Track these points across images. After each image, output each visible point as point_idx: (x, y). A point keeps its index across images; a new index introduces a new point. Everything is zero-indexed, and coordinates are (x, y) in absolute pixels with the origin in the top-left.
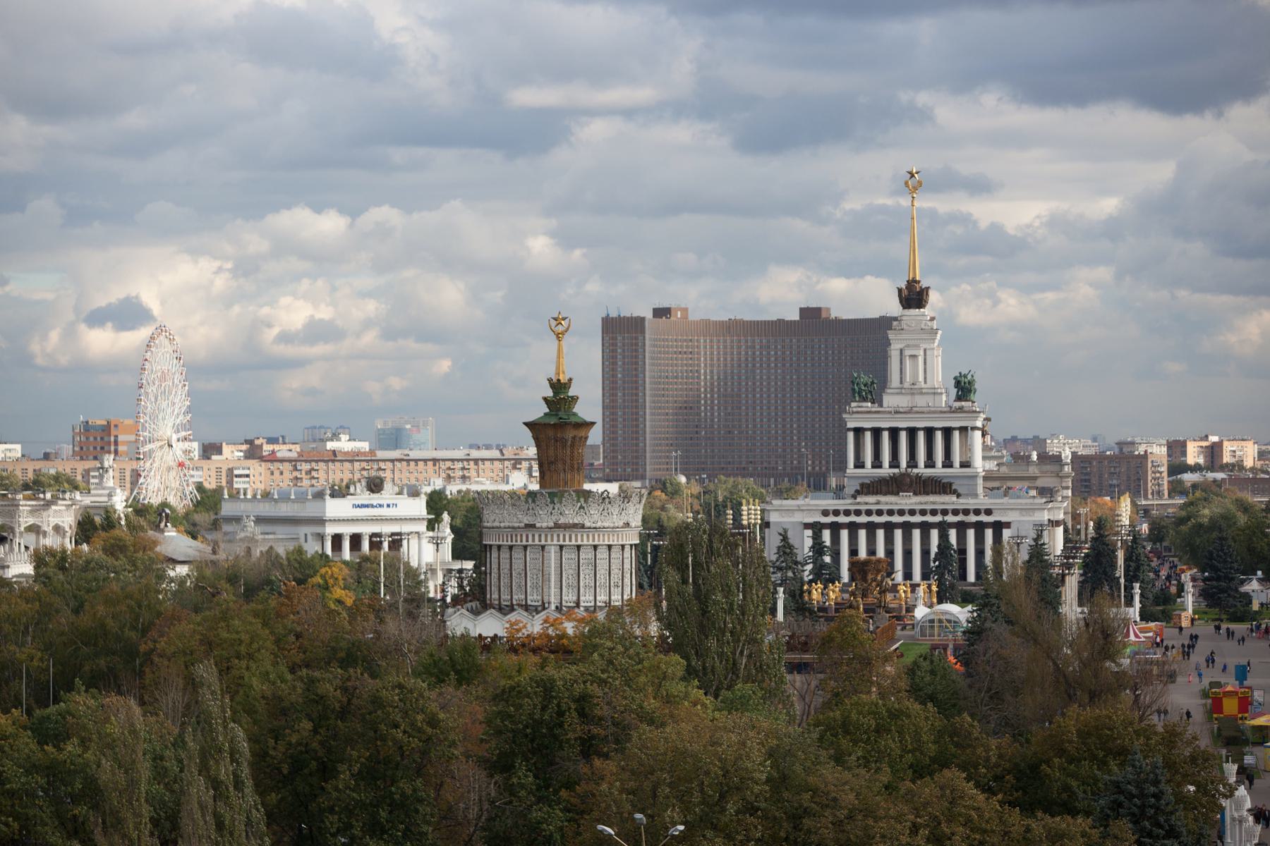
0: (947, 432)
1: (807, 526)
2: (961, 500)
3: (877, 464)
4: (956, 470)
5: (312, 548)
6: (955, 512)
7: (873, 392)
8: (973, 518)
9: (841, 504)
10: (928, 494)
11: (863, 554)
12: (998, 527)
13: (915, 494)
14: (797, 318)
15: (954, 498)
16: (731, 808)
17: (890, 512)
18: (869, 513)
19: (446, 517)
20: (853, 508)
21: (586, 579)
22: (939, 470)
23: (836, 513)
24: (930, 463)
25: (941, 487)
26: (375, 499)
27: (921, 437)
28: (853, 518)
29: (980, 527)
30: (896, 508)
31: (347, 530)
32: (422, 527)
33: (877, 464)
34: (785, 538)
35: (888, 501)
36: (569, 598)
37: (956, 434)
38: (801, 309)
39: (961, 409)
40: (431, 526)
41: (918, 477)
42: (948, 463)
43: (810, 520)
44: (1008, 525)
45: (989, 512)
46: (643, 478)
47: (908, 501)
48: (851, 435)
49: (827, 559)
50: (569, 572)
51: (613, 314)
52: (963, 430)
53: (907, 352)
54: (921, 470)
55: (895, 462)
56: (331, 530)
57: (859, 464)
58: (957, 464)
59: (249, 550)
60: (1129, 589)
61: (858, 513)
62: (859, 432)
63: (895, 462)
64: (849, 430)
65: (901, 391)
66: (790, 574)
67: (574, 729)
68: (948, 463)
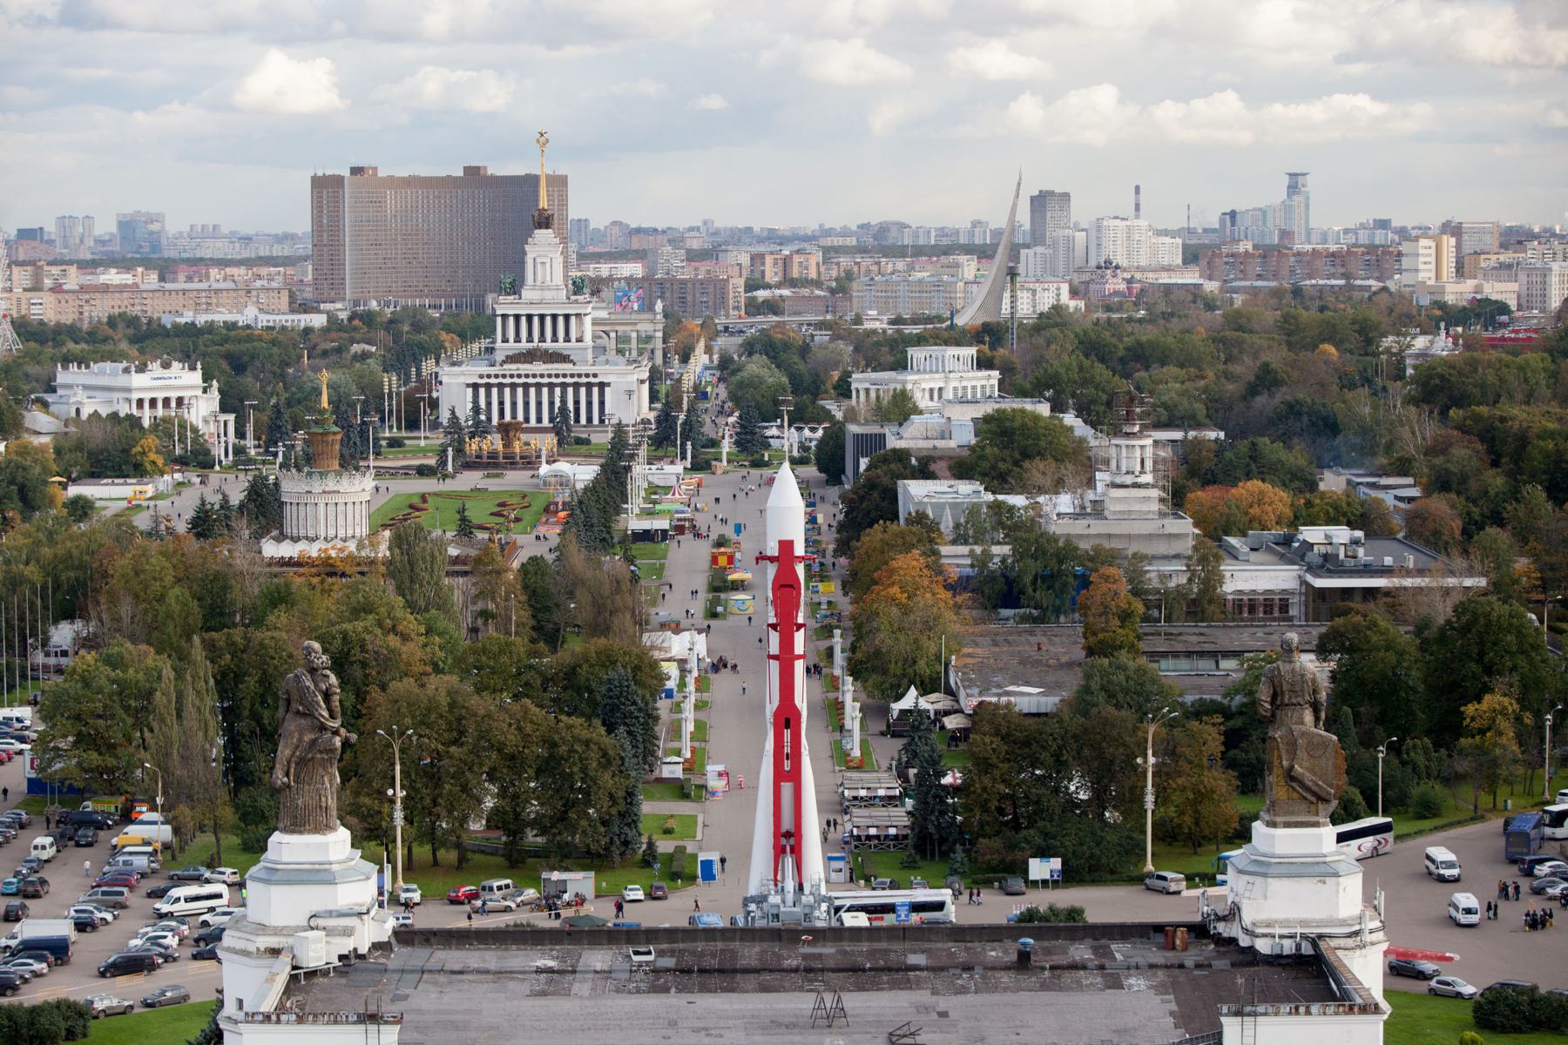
0: (567, 317)
1: (468, 385)
3: (517, 340)
4: (573, 344)
5: (123, 410)
6: (572, 376)
7: (515, 288)
8: (584, 380)
9: (492, 371)
11: (508, 418)
12: (602, 386)
14: (461, 174)
16: (433, 717)
17: (527, 376)
18: (512, 376)
19: (215, 383)
21: (341, 521)
22: (560, 345)
23: (489, 376)
24: (555, 339)
25: (565, 359)
26: (166, 373)
27: (548, 320)
28: (500, 380)
29: (589, 386)
31: (147, 396)
32: (199, 392)
33: (517, 340)
34: (453, 412)
35: (525, 368)
36: (331, 533)
37: (573, 319)
38: (466, 169)
39: (576, 302)
40: (205, 391)
41: (546, 351)
42: (567, 339)
44: (609, 384)
45: (595, 376)
46: (344, 299)
47: (538, 367)
48: (499, 320)
49: (483, 417)
50: (331, 518)
51: (320, 174)
53: (539, 260)
54: (548, 345)
55: (530, 340)
56: (135, 396)
57: (505, 340)
59: (78, 411)
60: (683, 445)
61: (504, 376)
62: (505, 317)
63: (530, 340)
65: (534, 288)
67: (356, 654)
68: (567, 339)
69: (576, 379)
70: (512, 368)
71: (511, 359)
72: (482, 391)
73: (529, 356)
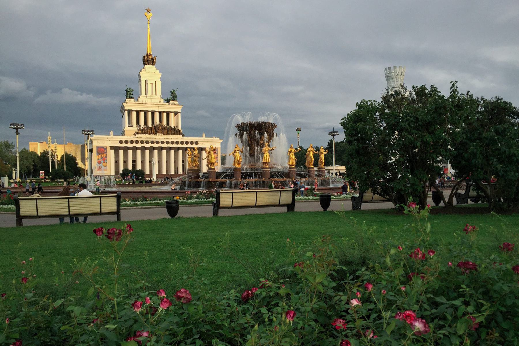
0: (168, 113)
1: (112, 148)
2: (184, 138)
6: (182, 143)
10: (169, 134)
13: (164, 134)
15: (181, 136)
17: (152, 142)
18: (142, 142)
20: (134, 140)
28: (134, 145)
30: (155, 140)
43: (114, 145)
44: (205, 149)
45: (197, 143)
47: (160, 137)
48: (126, 112)
53: (148, 82)
61: (137, 142)
64: (125, 110)
69: (185, 145)
72: (121, 152)
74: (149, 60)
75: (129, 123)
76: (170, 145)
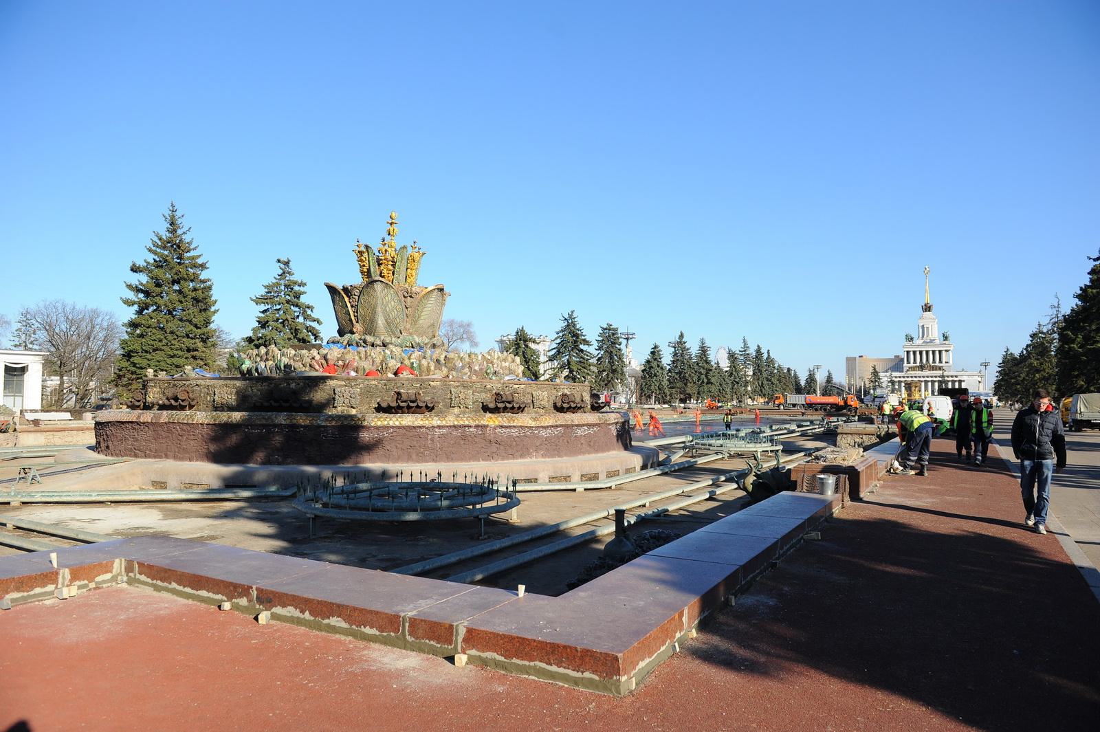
0: (940, 352)
17: (920, 377)
18: (912, 377)
22: (937, 364)
23: (900, 377)
25: (940, 368)
42: (940, 361)
44: (964, 381)
45: (956, 377)
47: (926, 373)
52: (946, 351)
53: (925, 326)
58: (944, 362)
61: (908, 377)
66: (877, 384)
68: (940, 361)
70: (913, 373)
71: (912, 369)
73: (922, 368)
74: (927, 308)
75: (908, 361)
76: (934, 379)
